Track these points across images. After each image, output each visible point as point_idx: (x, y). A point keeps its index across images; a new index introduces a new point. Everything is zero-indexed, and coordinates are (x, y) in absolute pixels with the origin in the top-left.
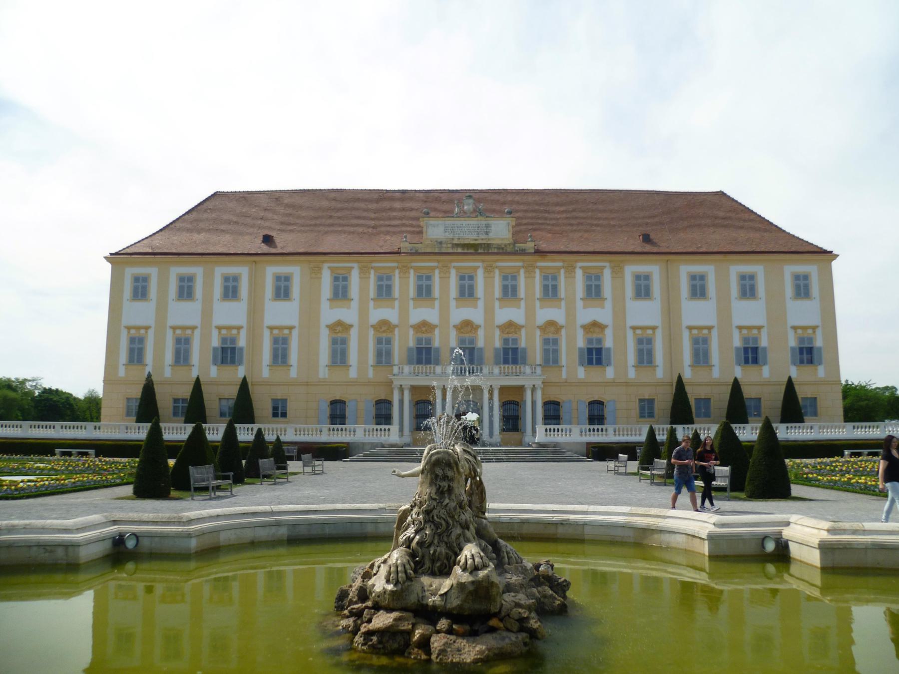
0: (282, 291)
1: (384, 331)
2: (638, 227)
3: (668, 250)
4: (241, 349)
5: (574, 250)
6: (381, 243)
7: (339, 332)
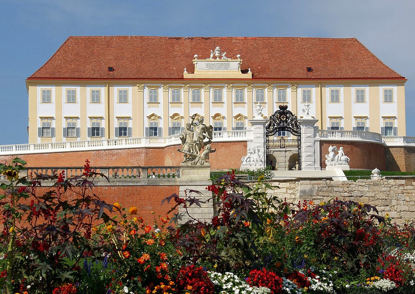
0: (123, 99)
1: (176, 119)
2: (306, 62)
3: (320, 77)
4: (102, 129)
5: (272, 77)
6: (172, 72)
7: (153, 120)
